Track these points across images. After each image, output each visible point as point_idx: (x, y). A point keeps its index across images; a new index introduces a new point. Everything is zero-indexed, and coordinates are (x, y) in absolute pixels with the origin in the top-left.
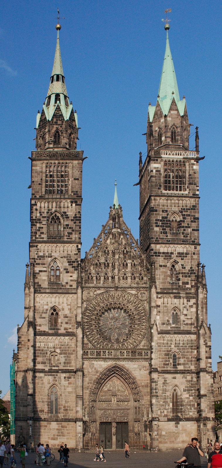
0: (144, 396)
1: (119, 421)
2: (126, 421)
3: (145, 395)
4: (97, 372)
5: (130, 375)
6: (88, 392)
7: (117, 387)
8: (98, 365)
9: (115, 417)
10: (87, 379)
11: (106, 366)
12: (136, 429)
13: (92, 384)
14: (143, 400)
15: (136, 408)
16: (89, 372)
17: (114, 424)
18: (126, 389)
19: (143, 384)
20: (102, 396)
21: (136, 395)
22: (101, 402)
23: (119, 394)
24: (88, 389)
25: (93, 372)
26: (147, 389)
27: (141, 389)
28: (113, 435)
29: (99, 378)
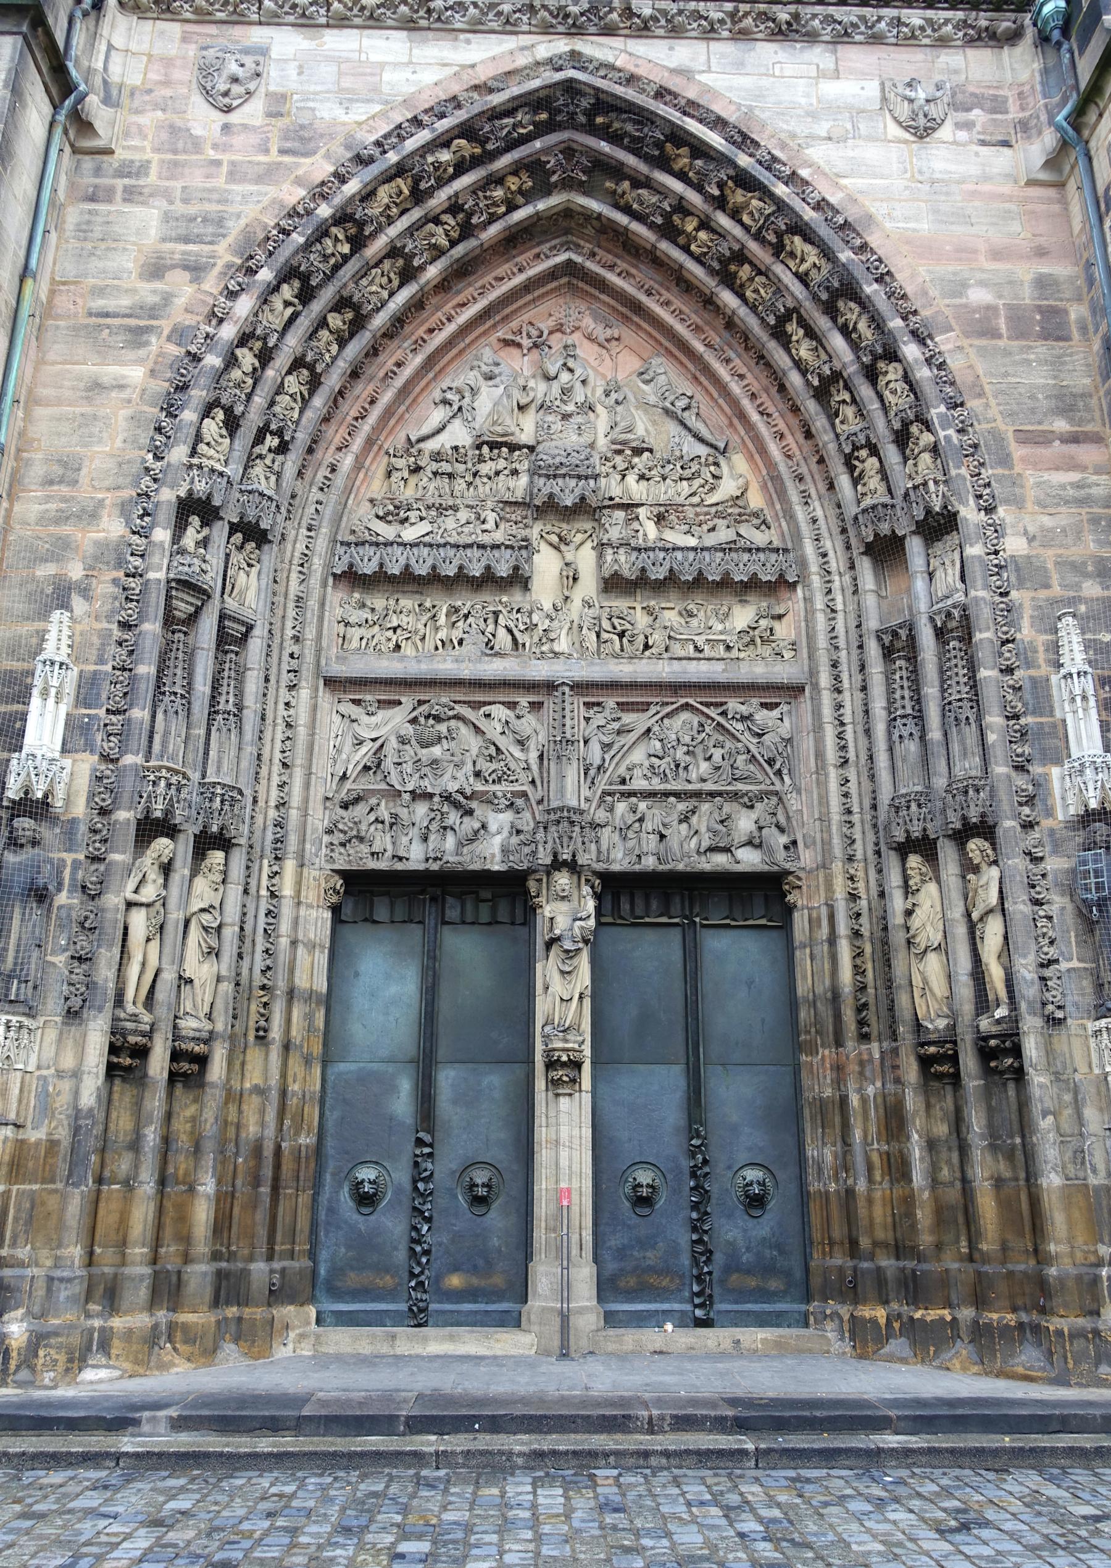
0: (1018, 452)
1: (649, 863)
2: (749, 860)
3: (1042, 439)
4: (301, 140)
5: (781, 190)
6: (136, 374)
7: (602, 420)
8: (327, 72)
9: (572, 789)
10: (144, 224)
11: (429, 77)
12: (933, 964)
13: (212, 284)
14: (1018, 502)
15: (898, 645)
16: (177, 138)
17: (566, 910)
18: (736, 436)
19: (978, 296)
20: (397, 514)
21: (891, 453)
22: (379, 602)
23: (636, 489)
24: (137, 336)
25: (238, 140)
26: (1057, 363)
27: (955, 363)
28: (540, 1084)
29: (324, 211)
